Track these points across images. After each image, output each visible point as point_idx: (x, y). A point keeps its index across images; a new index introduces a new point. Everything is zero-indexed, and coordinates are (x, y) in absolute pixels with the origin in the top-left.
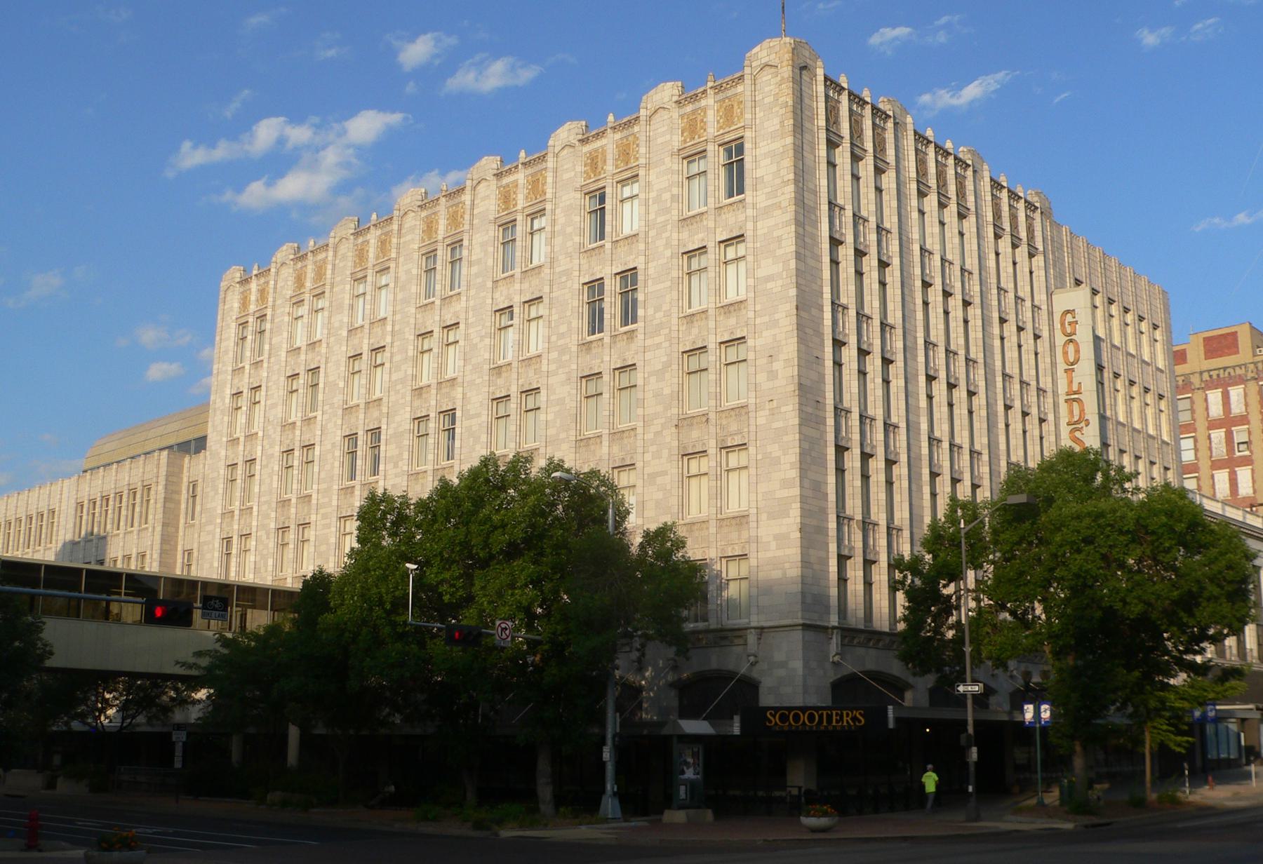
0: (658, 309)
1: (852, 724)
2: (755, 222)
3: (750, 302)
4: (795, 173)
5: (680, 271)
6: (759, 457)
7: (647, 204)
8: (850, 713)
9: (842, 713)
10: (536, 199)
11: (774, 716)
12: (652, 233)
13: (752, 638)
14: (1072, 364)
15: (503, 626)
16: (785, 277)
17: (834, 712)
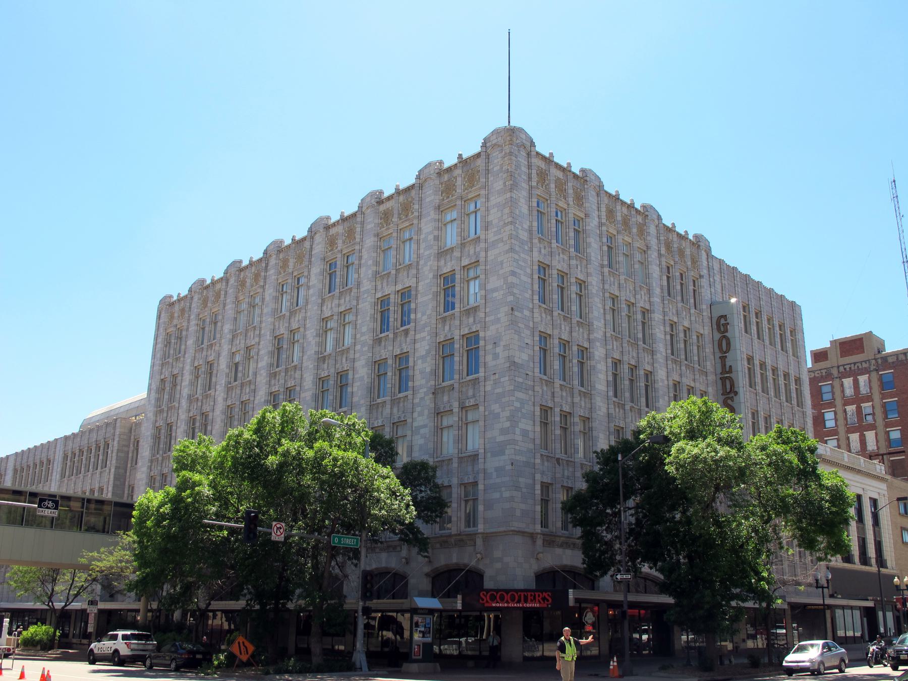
0: (423, 314)
2: (486, 252)
3: (482, 307)
5: (439, 288)
6: (487, 413)
7: (418, 242)
8: (541, 595)
9: (535, 595)
10: (350, 242)
11: (486, 596)
12: (421, 262)
13: (479, 542)
14: (725, 353)
16: (505, 288)
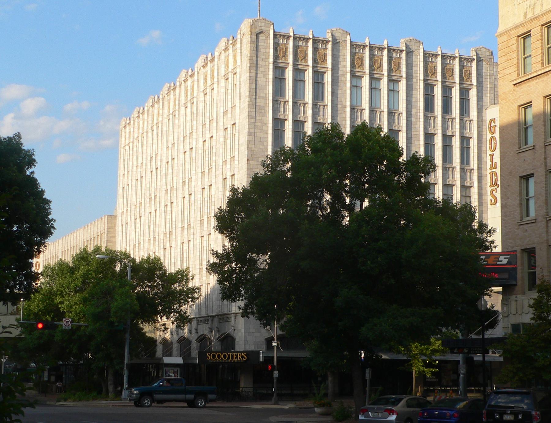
1: (241, 359)
4: (249, 92)
9: (237, 355)
11: (210, 355)
15: (67, 320)
17: (234, 354)
